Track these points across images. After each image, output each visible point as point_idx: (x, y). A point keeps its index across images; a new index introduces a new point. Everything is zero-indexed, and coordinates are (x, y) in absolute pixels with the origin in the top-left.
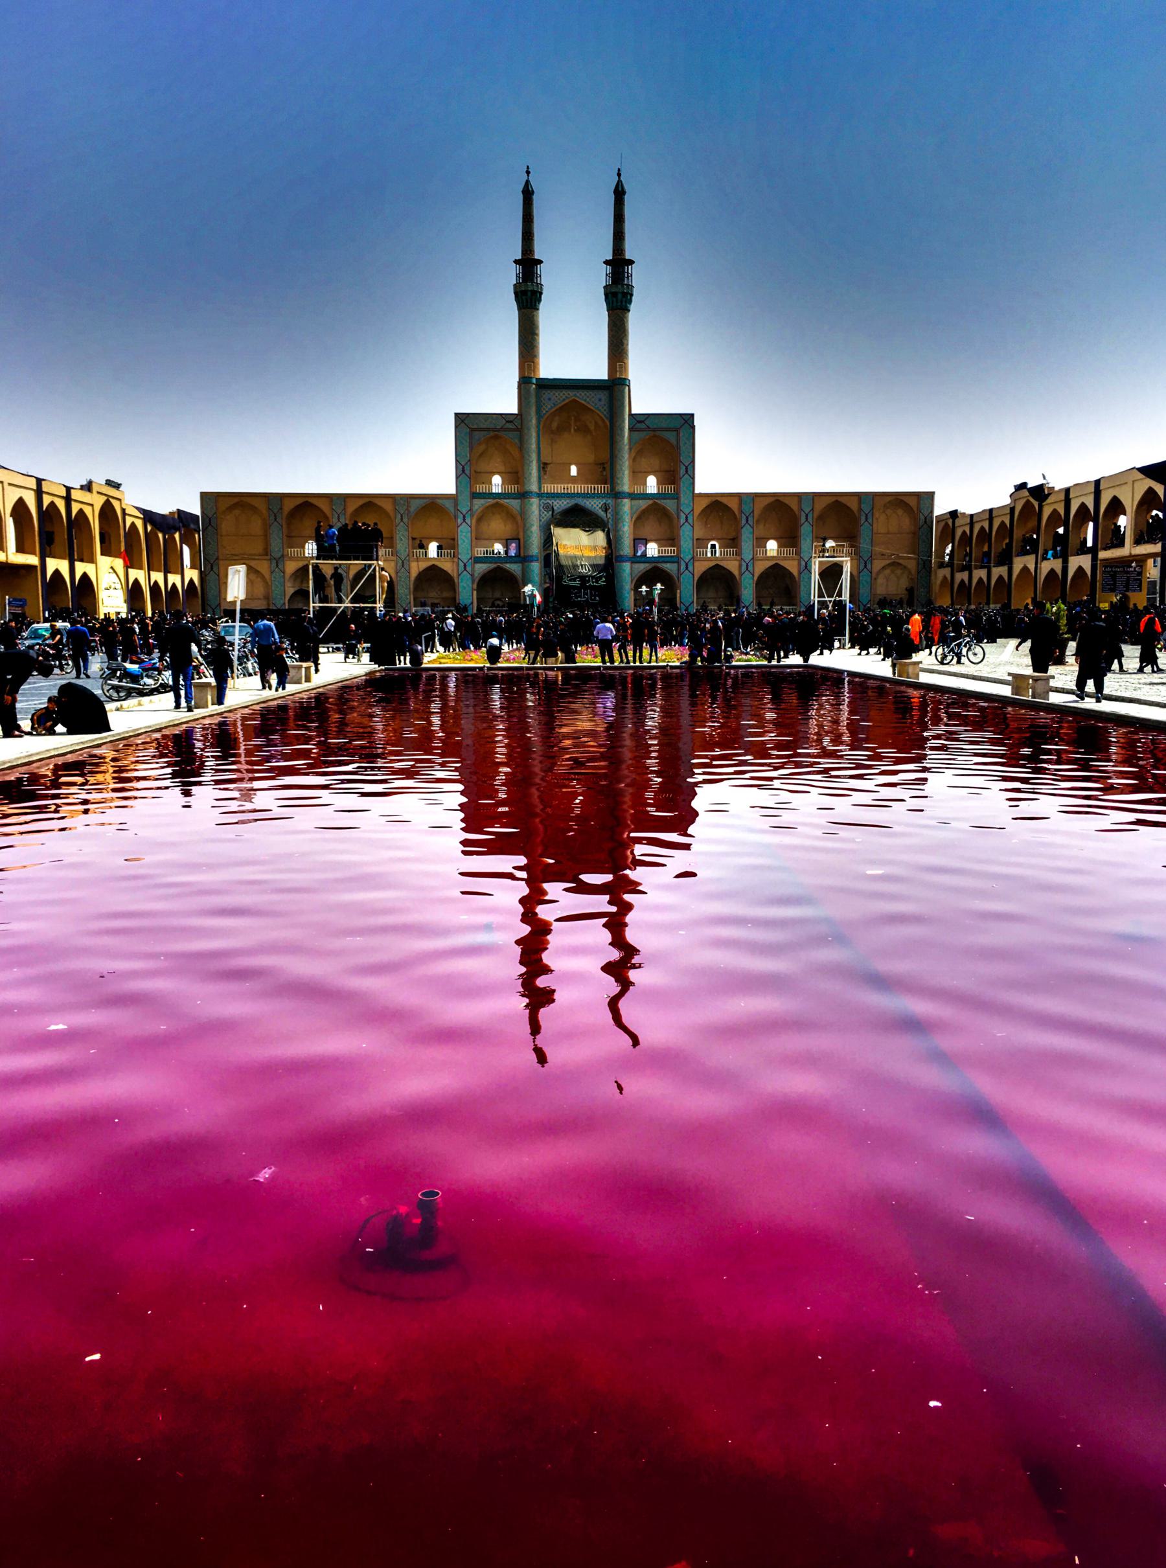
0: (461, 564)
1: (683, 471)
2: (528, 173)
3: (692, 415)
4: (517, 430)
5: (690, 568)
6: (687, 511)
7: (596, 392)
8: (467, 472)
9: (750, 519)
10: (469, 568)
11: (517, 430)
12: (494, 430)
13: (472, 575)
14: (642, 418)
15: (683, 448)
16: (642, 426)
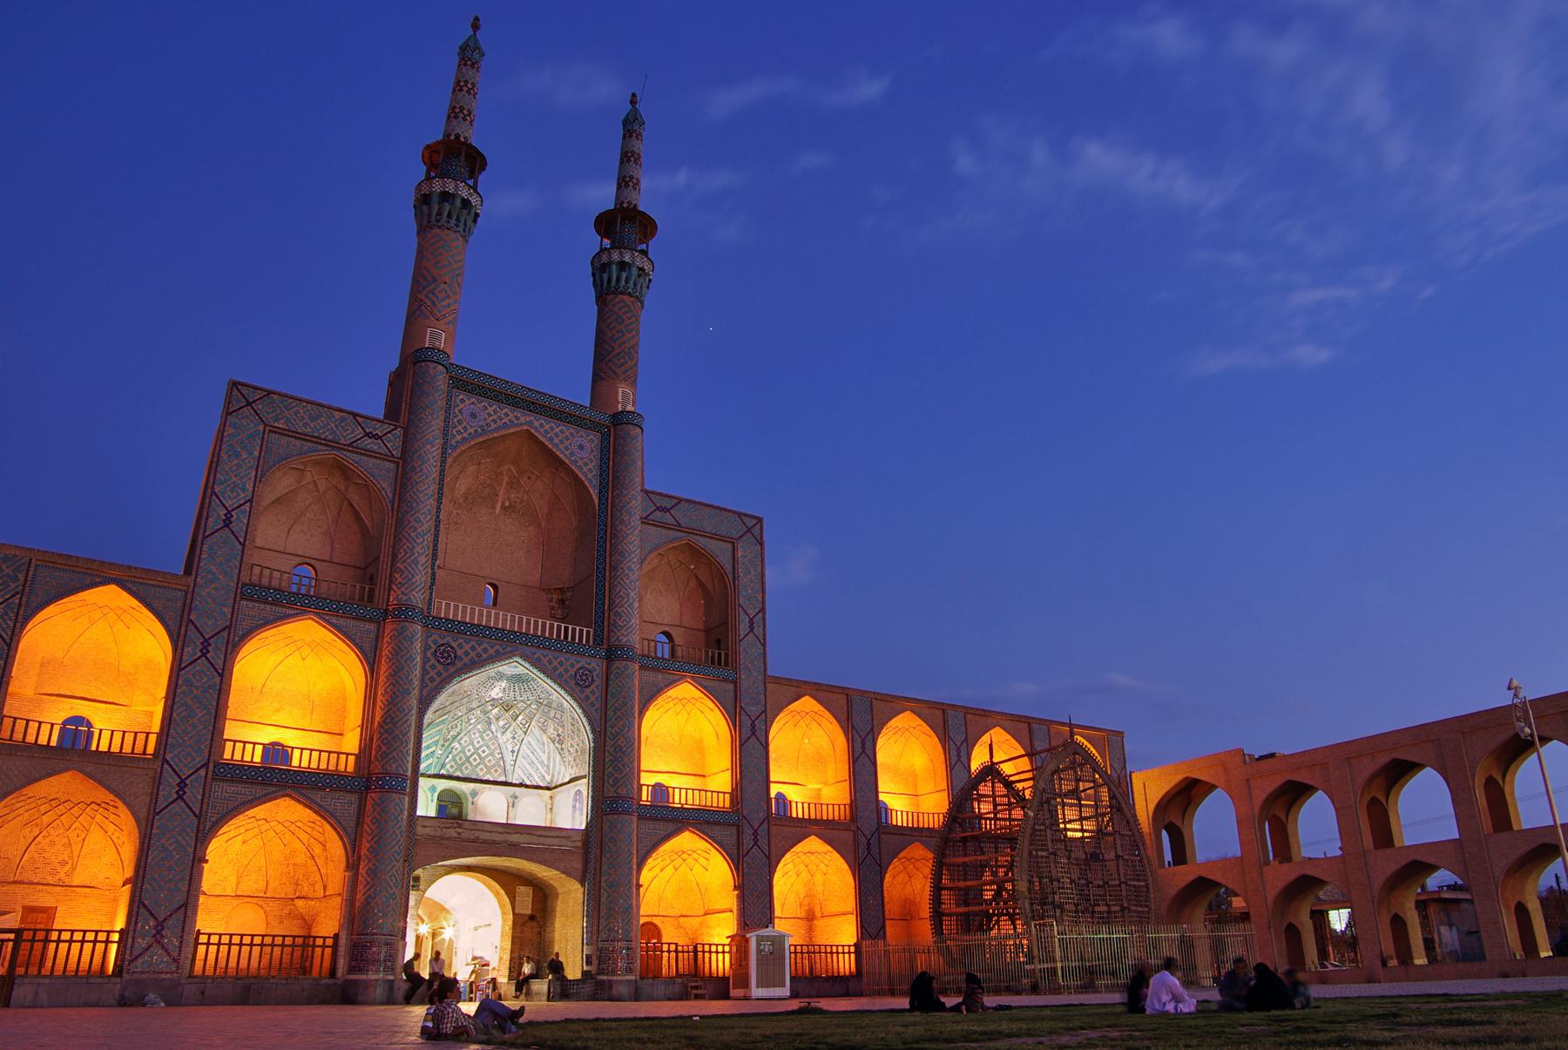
0: (171, 780)
1: (743, 628)
2: (476, 26)
3: (760, 520)
4: (388, 457)
5: (763, 842)
6: (754, 710)
7: (573, 429)
8: (238, 525)
9: (868, 744)
10: (193, 794)
11: (388, 457)
12: (333, 444)
13: (198, 817)
14: (667, 503)
15: (746, 580)
16: (668, 518)
